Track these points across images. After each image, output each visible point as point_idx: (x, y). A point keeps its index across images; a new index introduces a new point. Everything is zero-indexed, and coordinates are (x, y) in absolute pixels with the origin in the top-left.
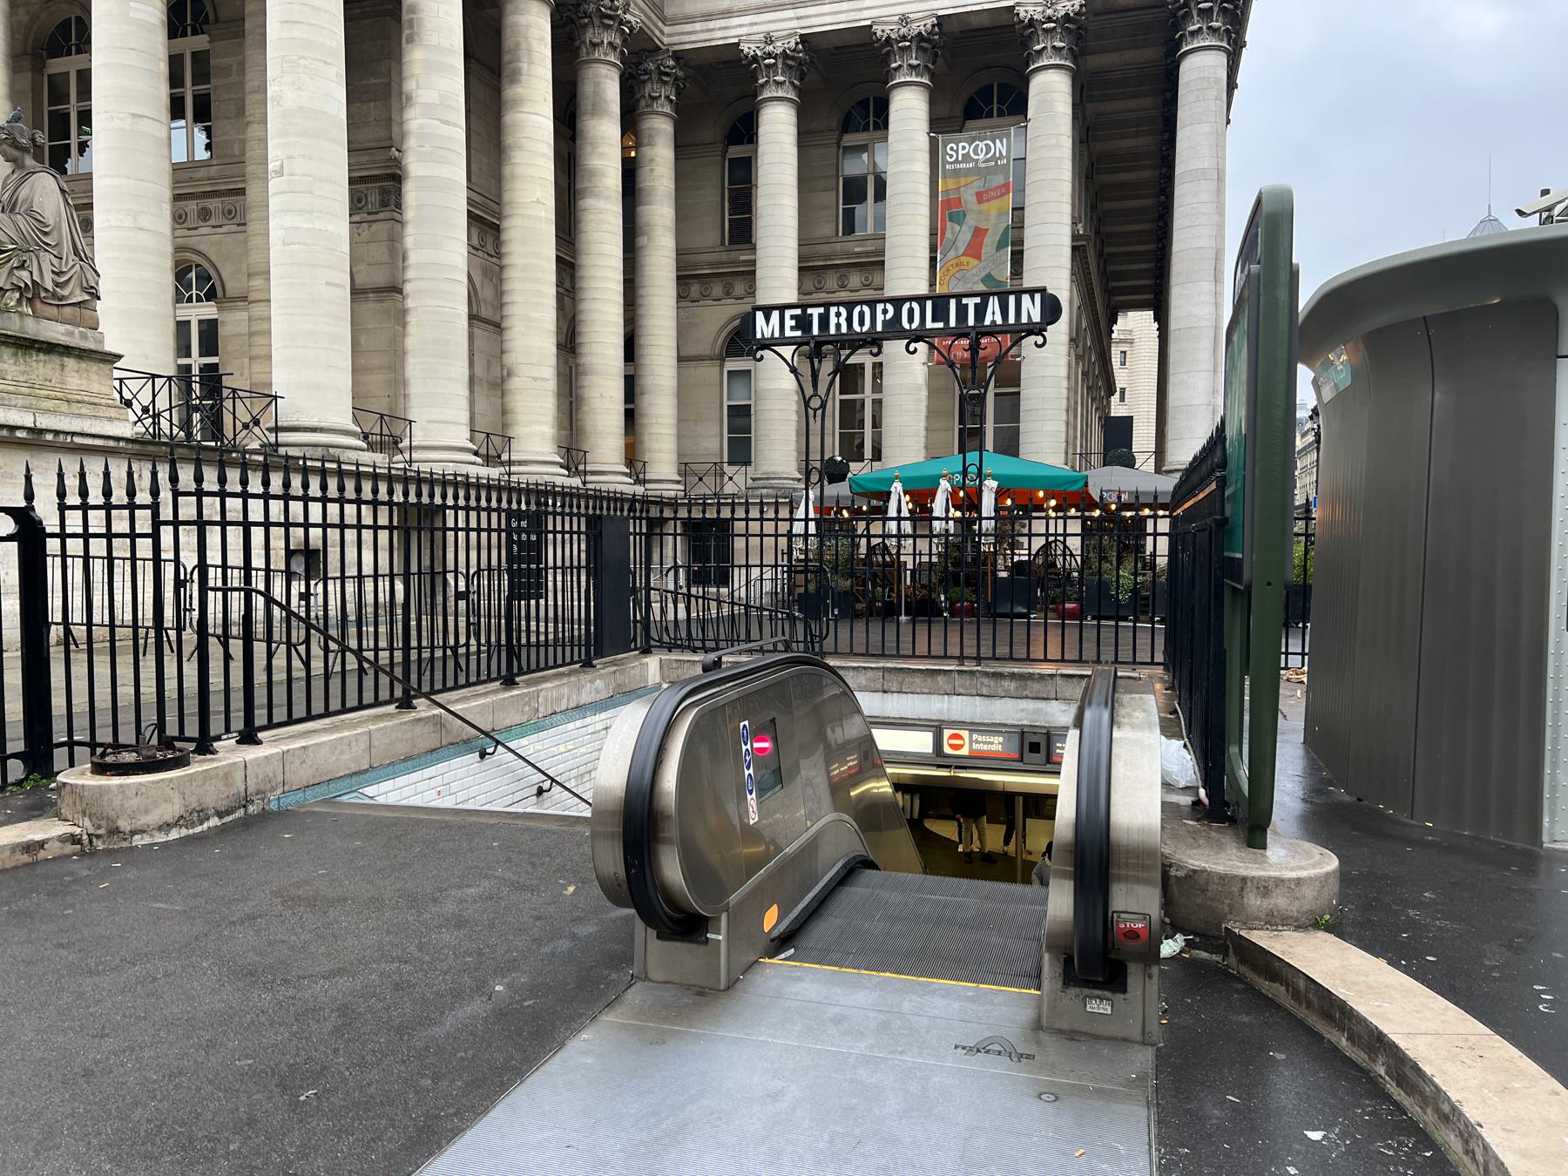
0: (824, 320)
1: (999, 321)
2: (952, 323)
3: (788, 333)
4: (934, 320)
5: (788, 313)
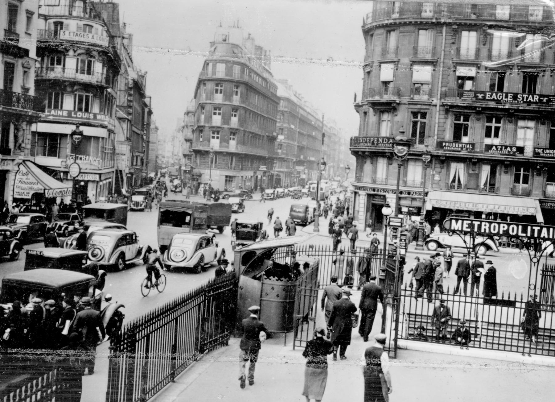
0: (480, 227)
1: (546, 237)
2: (529, 235)
3: (465, 229)
4: (522, 232)
5: (465, 222)
